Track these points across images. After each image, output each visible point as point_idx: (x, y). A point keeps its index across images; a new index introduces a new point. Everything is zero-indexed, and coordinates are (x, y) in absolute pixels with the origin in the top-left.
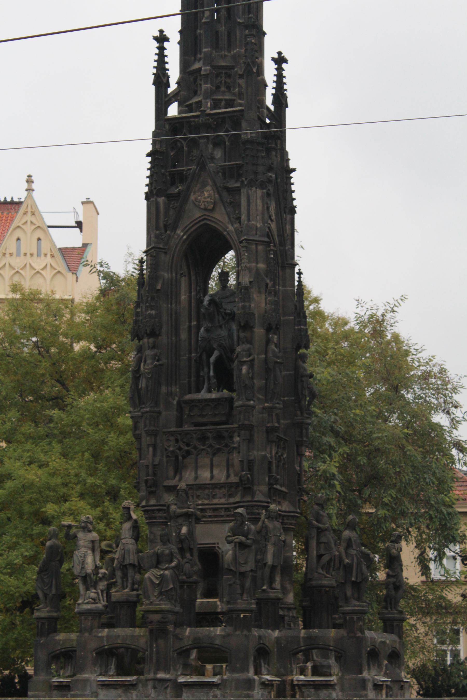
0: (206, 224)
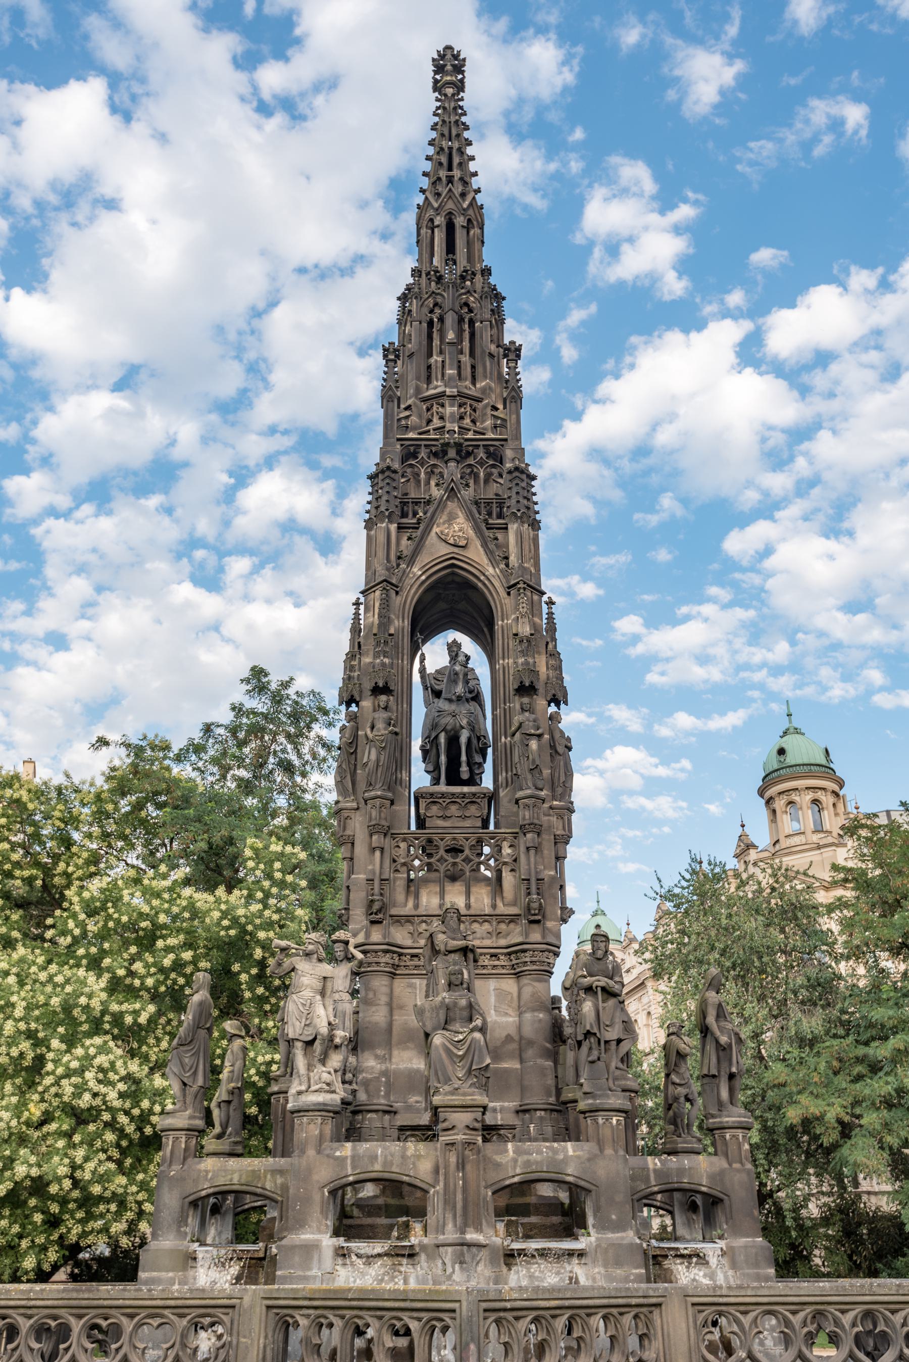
0: (453, 565)
